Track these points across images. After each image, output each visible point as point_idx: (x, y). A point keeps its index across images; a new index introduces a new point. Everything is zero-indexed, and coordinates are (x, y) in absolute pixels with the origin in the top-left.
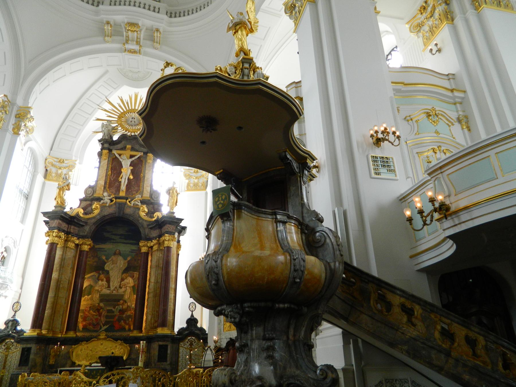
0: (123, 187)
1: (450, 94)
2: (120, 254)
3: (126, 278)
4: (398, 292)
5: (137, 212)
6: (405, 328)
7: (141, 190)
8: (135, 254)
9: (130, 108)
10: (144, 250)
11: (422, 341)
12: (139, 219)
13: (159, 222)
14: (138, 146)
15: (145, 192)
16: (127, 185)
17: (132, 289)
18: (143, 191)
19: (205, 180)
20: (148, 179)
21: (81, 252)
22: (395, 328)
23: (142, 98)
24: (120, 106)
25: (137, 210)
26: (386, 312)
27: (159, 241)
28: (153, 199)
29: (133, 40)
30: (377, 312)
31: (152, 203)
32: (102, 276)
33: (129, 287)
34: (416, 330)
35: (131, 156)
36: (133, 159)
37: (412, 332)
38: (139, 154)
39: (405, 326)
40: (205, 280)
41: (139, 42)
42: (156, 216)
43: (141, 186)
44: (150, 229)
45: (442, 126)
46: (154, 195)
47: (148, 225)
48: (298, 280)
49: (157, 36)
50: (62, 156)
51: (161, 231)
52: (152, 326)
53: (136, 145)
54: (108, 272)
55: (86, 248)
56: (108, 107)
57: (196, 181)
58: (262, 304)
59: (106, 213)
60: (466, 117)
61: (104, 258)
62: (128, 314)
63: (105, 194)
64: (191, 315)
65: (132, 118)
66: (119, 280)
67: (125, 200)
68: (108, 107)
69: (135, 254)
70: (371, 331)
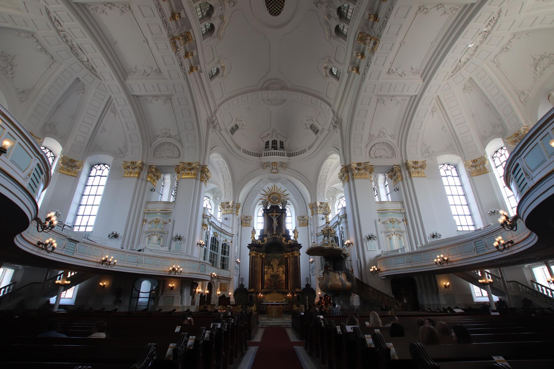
0: (275, 230)
1: (399, 211)
2: (276, 258)
19: (307, 221)
21: (262, 258)
24: (268, 192)
27: (292, 253)
32: (270, 267)
33: (281, 271)
45: (396, 224)
46: (287, 232)
50: (247, 215)
54: (272, 265)
55: (264, 256)
56: (264, 193)
57: (303, 222)
59: (270, 242)
60: (406, 219)
61: (270, 260)
63: (268, 234)
66: (277, 269)
68: (264, 193)
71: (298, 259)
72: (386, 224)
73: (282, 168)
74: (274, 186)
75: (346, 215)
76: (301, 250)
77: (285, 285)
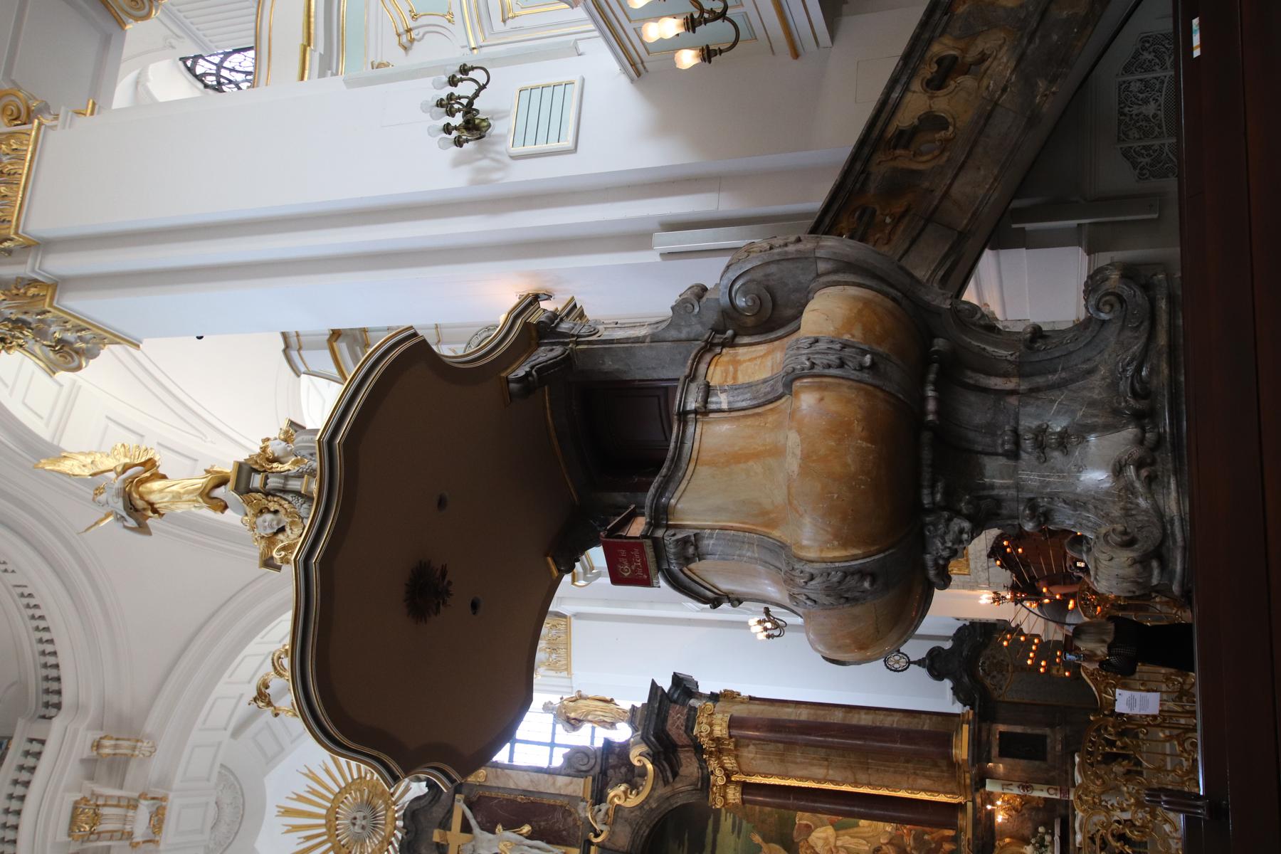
3: (813, 847)
4: (895, 95)
5: (626, 814)
6: (992, 82)
7: (566, 801)
8: (744, 823)
9: (324, 830)
10: (734, 795)
11: (1025, 41)
12: (646, 807)
13: (659, 752)
14: (434, 809)
15: (569, 791)
16: (549, 842)
17: (841, 832)
18: (566, 796)
20: (532, 781)
22: (989, 108)
23: (295, 797)
25: (620, 814)
26: (947, 129)
28: (592, 769)
29: (124, 819)
30: (947, 154)
31: (603, 772)
33: (837, 837)
34: (996, 55)
35: (466, 828)
36: (473, 822)
37: (1002, 65)
38: (460, 807)
39: (985, 82)
40: (857, 610)
41: (129, 799)
42: (639, 761)
43: (552, 802)
44: (677, 779)
46: (578, 762)
47: (666, 783)
48: (868, 359)
49: (116, 746)
51: (683, 746)
52: (946, 774)
53: (434, 815)
58: (927, 455)
62: (912, 843)
64: (920, 665)
65: (354, 824)
67: (593, 848)
69: (744, 823)
70: (996, 171)
71: (756, 709)
72: (415, 17)
73: (133, 764)
74: (288, 812)
75: (336, 335)
76: (706, 686)
77: (927, 829)
